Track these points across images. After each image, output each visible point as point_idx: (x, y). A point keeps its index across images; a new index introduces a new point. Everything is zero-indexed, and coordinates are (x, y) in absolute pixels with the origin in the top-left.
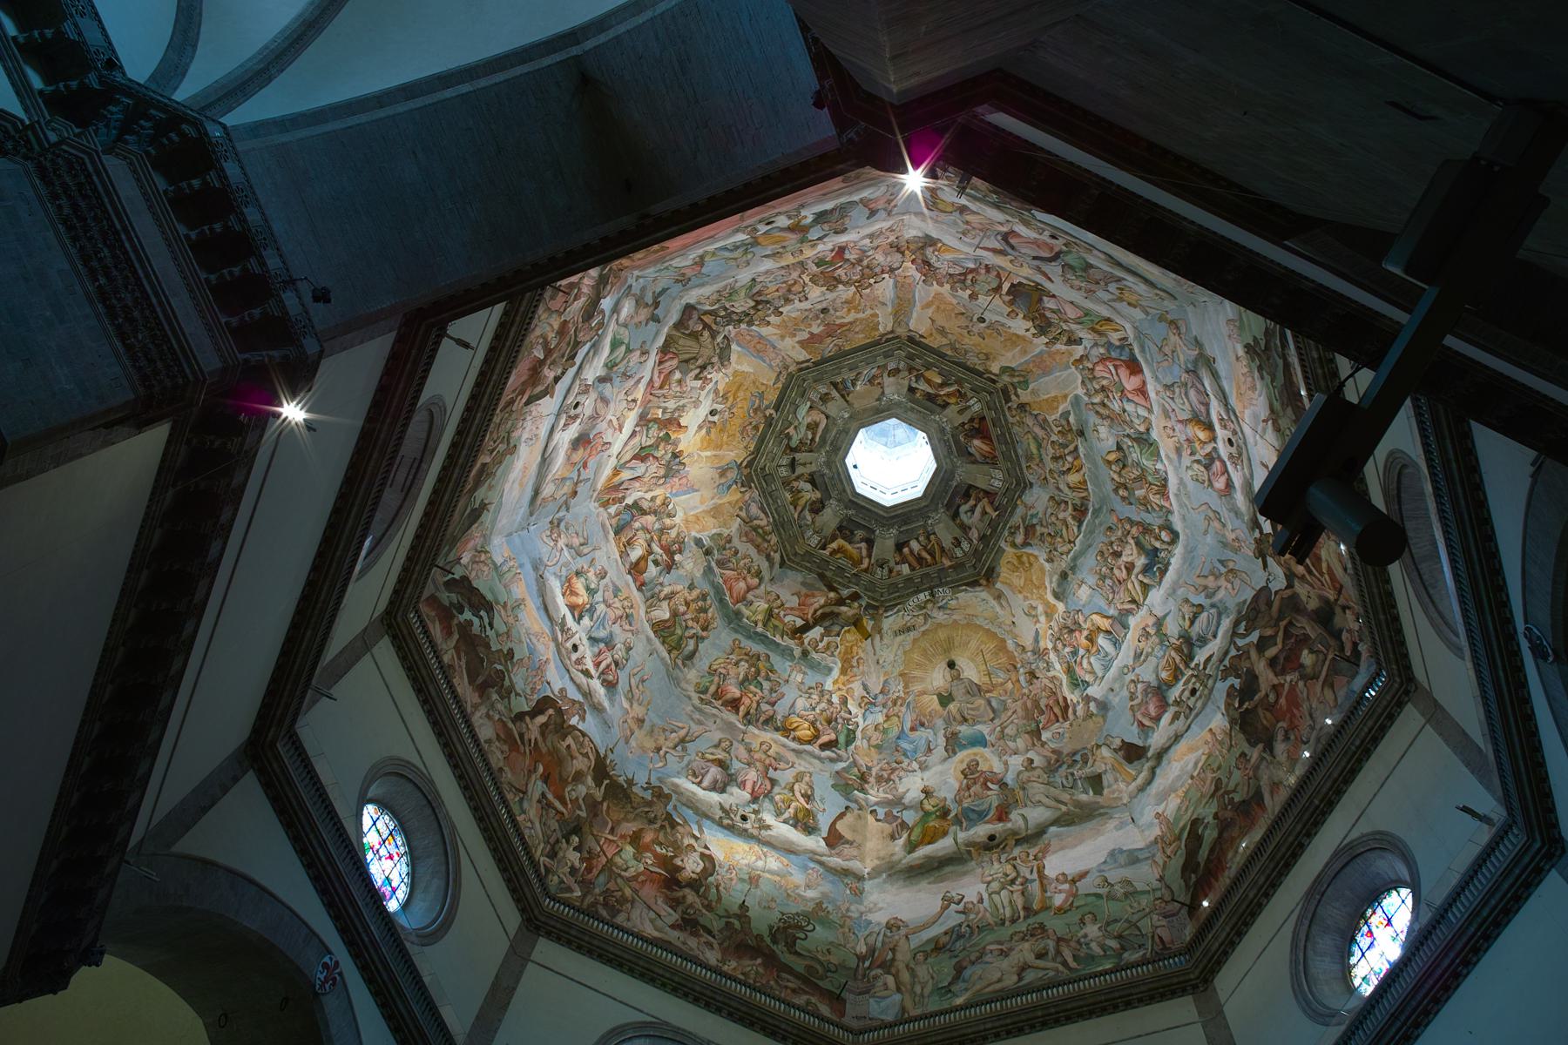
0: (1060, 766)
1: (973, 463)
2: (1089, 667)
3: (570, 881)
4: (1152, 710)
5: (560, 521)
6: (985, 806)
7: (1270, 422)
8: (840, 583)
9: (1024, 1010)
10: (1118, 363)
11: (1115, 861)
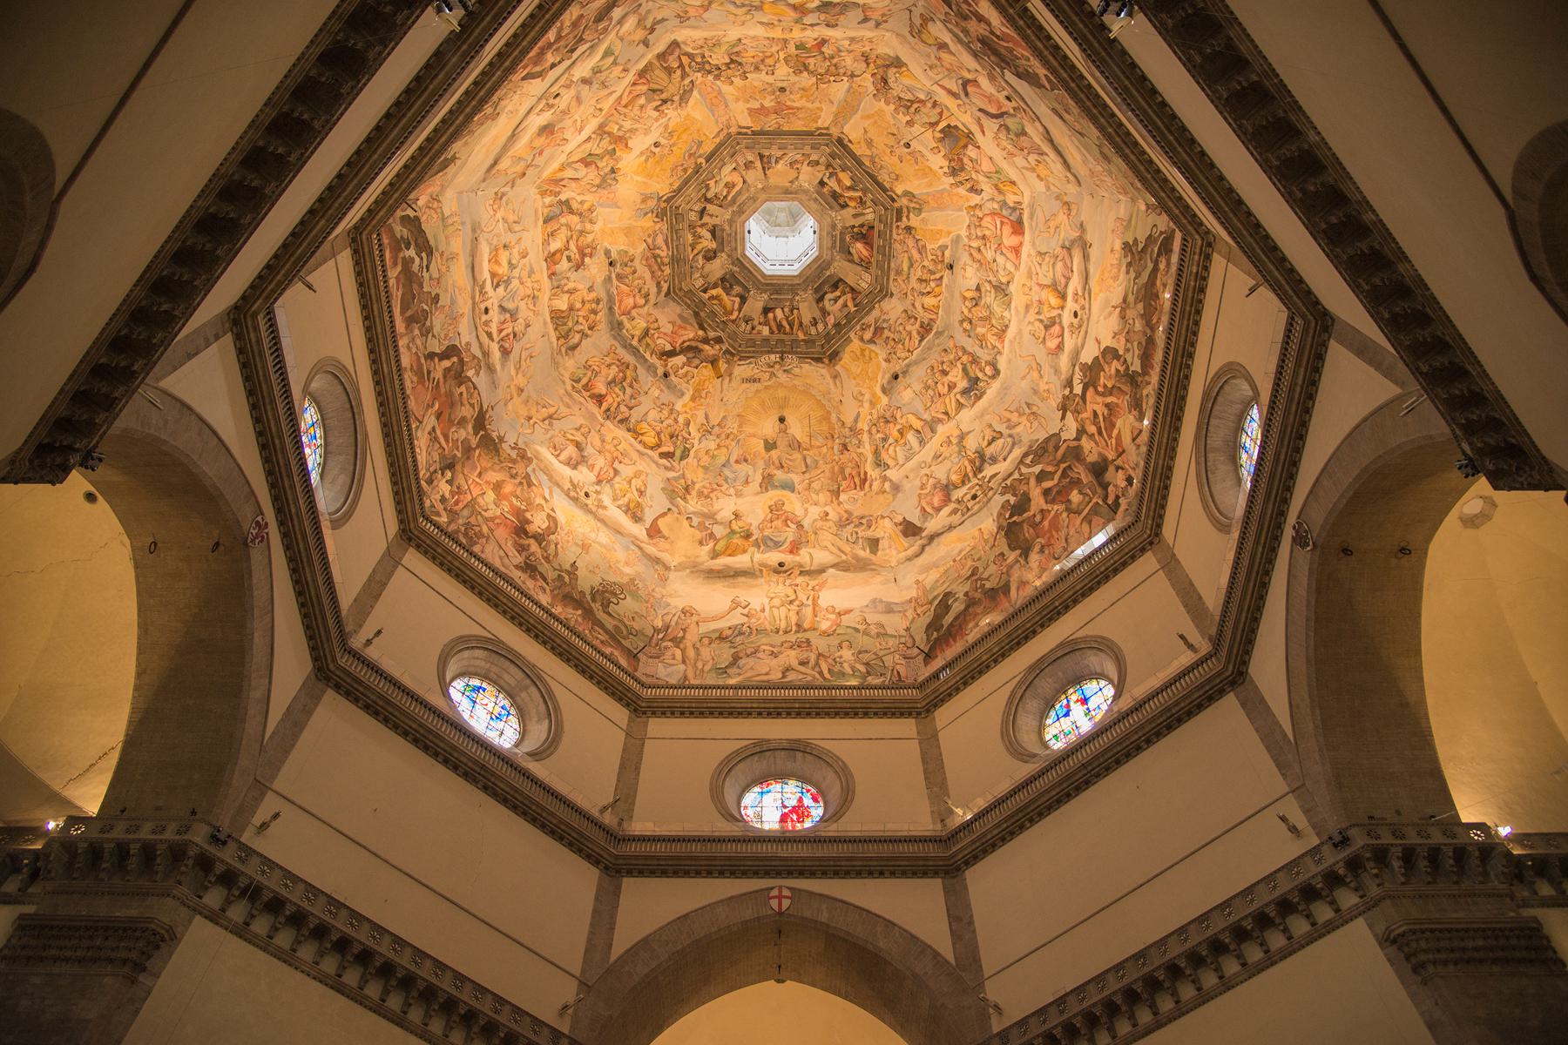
0: (849, 524)
1: (849, 261)
3: (440, 507)
5: (503, 195)
6: (782, 539)
7: (1118, 310)
8: (709, 325)
9: (785, 700)
10: (1005, 220)
11: (875, 607)
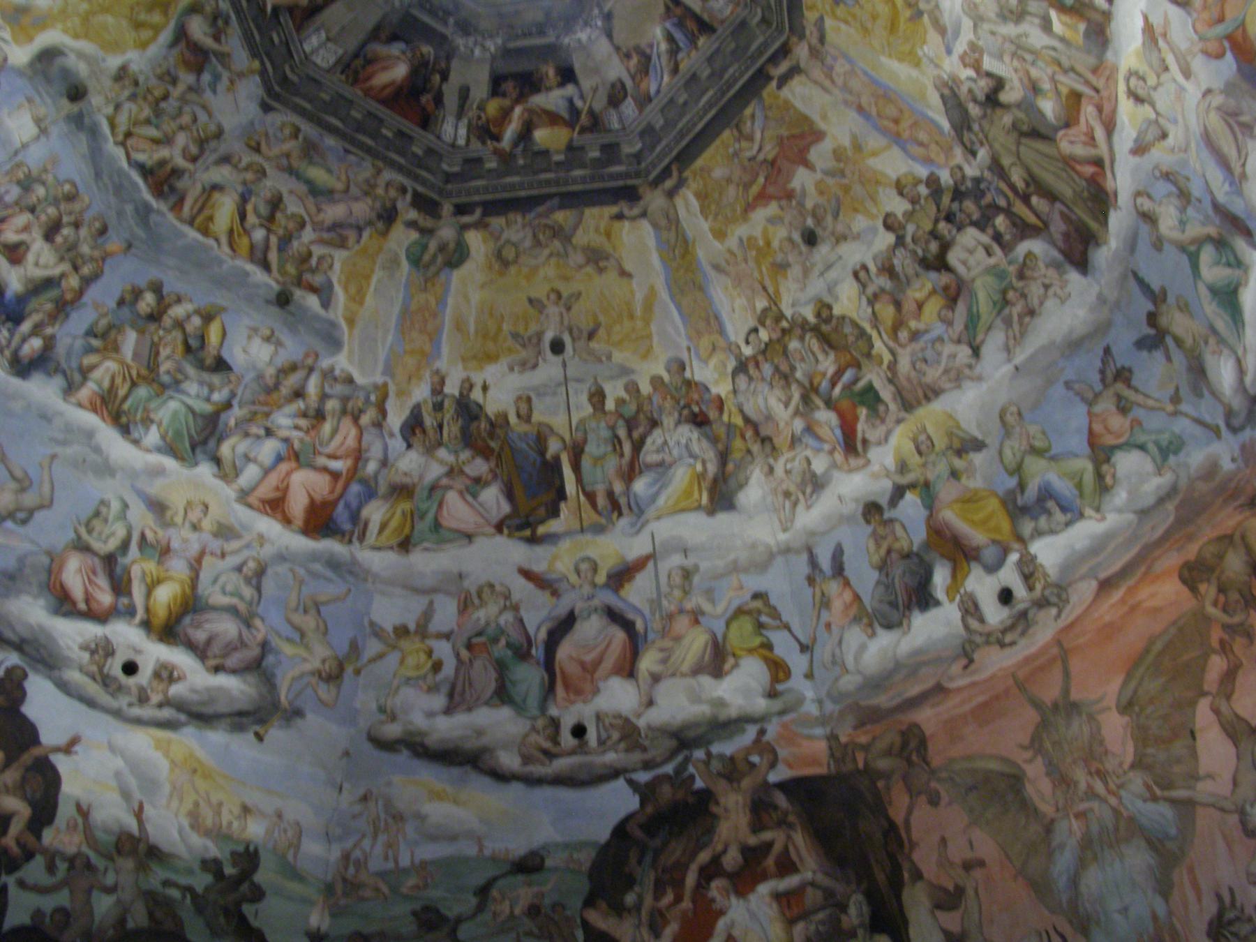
7: (132, 824)
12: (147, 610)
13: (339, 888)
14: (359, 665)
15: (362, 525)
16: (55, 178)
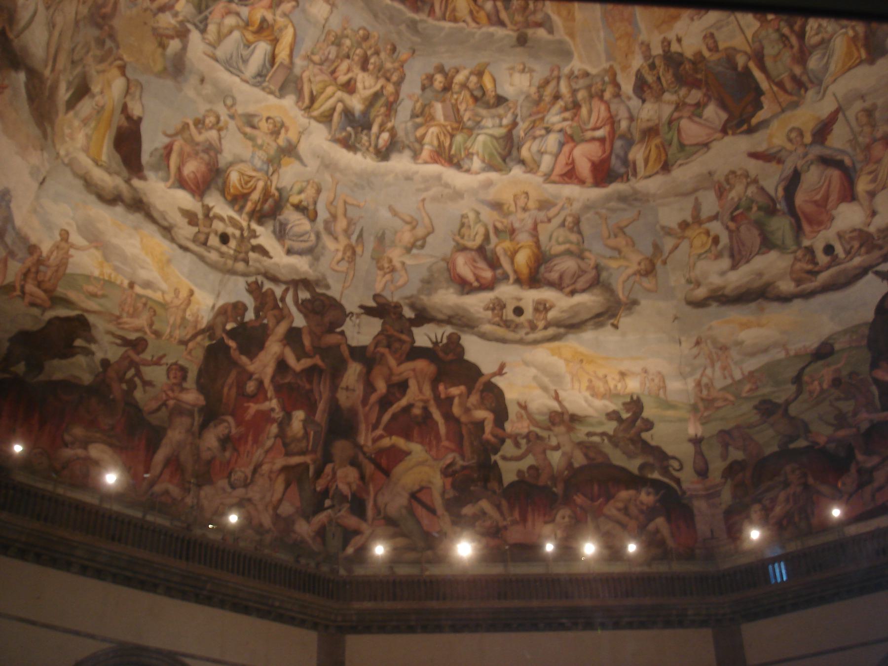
2: (225, 30)
4: (191, 168)
7: (555, 406)
12: (515, 272)
13: (701, 405)
14: (664, 257)
15: (632, 165)
16: (352, 30)
